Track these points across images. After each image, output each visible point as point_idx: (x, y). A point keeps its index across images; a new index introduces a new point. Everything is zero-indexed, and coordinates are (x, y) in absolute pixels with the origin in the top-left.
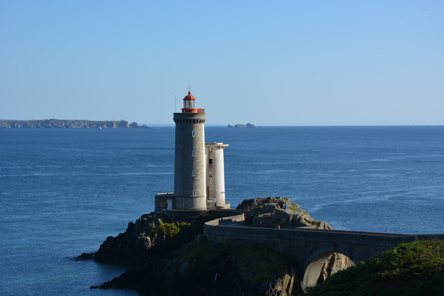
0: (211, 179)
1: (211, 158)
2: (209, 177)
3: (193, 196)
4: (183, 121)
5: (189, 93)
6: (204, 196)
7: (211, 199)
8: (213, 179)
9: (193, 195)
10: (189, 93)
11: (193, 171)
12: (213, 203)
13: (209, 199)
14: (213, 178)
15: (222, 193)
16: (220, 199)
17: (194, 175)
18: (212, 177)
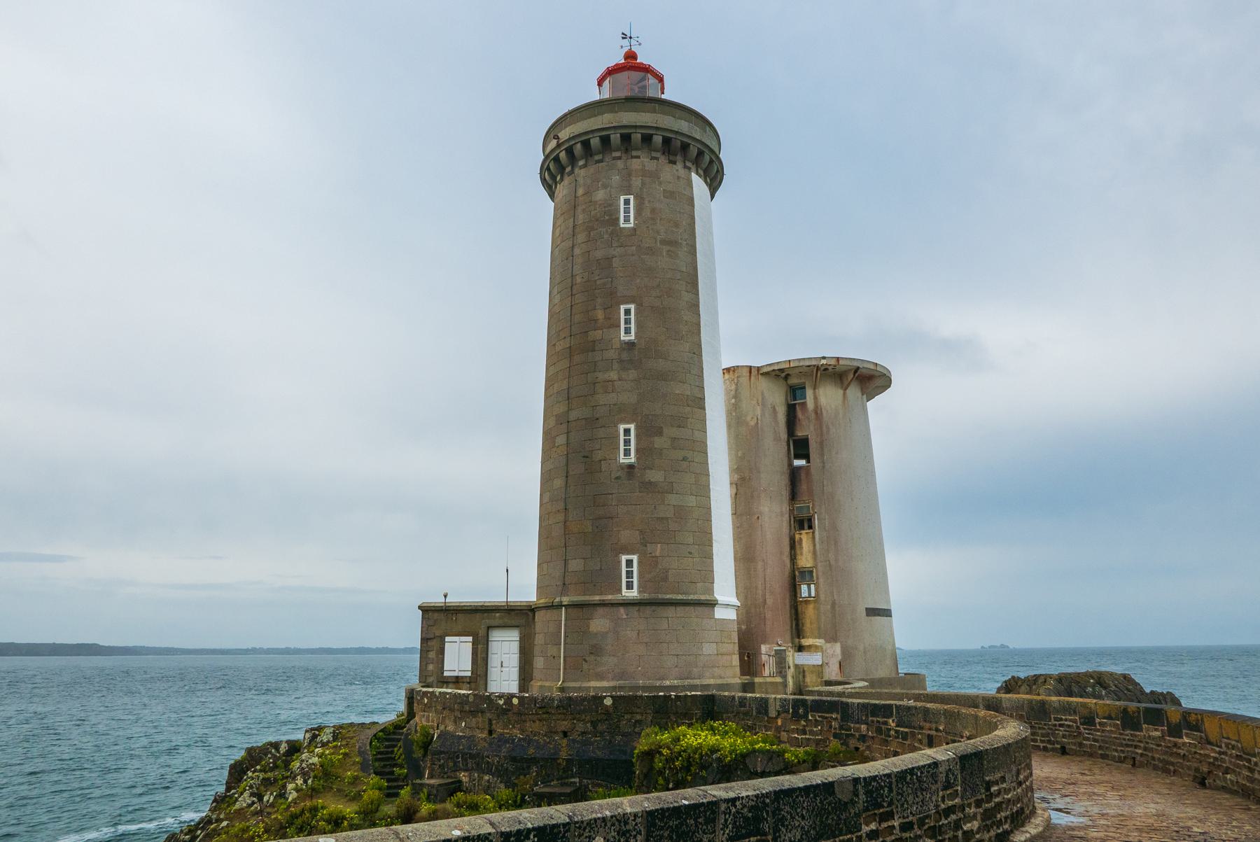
0: (804, 537)
1: (800, 433)
2: (802, 528)
3: (618, 597)
4: (570, 151)
5: (631, 56)
6: (712, 604)
7: (810, 646)
8: (814, 538)
9: (620, 591)
10: (631, 56)
11: (622, 427)
12: (821, 666)
13: (800, 649)
14: (813, 533)
15: (872, 612)
16: (861, 648)
17: (627, 453)
18: (810, 527)
